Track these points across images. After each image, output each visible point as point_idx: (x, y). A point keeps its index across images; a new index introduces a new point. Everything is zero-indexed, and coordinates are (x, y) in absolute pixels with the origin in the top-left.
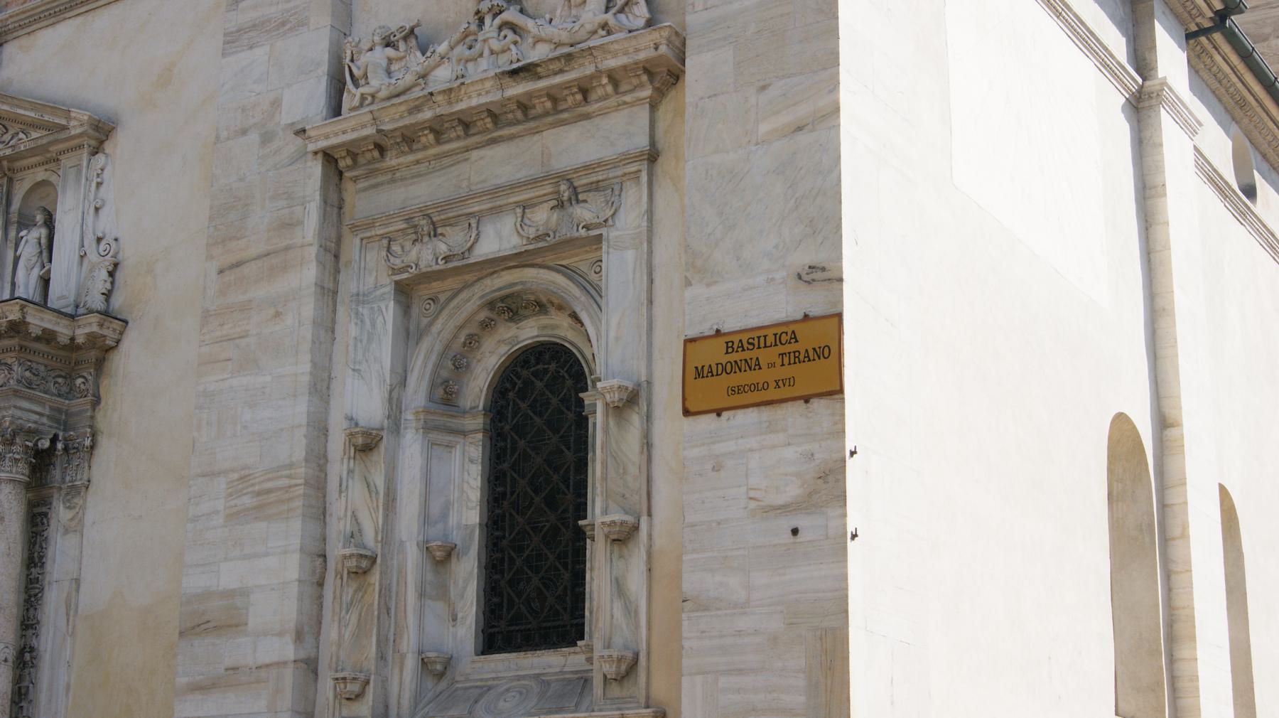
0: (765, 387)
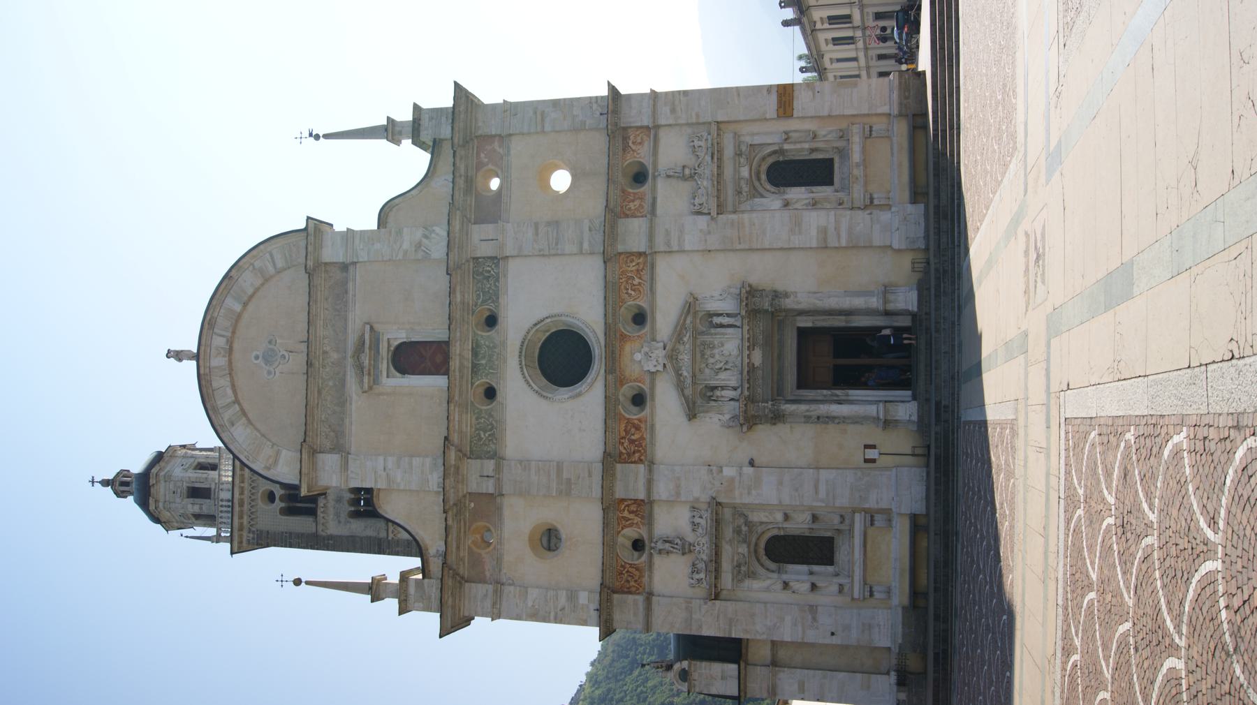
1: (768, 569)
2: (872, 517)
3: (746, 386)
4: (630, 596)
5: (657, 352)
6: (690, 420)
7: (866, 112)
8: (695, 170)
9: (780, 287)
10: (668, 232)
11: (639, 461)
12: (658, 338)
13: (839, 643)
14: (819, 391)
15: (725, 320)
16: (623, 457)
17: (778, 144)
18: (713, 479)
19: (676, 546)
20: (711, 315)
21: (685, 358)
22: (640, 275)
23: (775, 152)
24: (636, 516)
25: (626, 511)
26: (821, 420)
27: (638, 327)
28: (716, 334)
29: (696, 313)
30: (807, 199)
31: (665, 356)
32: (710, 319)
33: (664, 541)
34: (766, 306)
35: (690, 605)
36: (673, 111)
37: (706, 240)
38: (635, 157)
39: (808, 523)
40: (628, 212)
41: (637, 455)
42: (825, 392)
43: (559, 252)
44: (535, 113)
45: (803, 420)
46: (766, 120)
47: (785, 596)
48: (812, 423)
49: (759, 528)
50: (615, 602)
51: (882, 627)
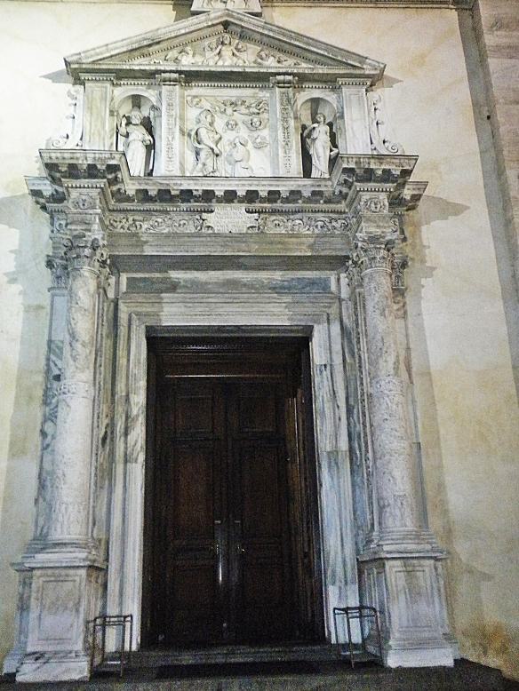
26: (55, 384)
28: (286, 129)
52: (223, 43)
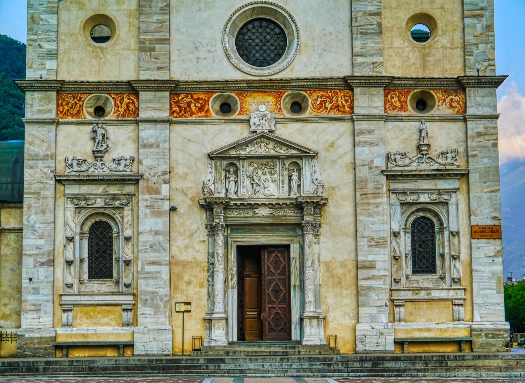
0: (487, 236)
1: (83, 224)
2: (131, 310)
3: (239, 203)
4: (54, 106)
5: (267, 124)
6: (209, 155)
7: (475, 302)
8: (426, 154)
9: (322, 231)
10: (370, 132)
11: (172, 111)
12: (279, 126)
13: (24, 285)
14: (236, 264)
15: (294, 184)
16: (175, 97)
17: (449, 227)
18: (159, 176)
19: (100, 145)
20: (299, 170)
21: (262, 149)
22: (334, 109)
23: (442, 224)
24: (125, 110)
25: (128, 101)
26: (211, 266)
27: (289, 107)
29: (300, 157)
30: (400, 251)
31: (263, 132)
32: (295, 170)
33: (104, 135)
34: (307, 219)
35: (50, 159)
36: (479, 134)
37: (364, 166)
38: (439, 101)
39: (123, 257)
40: (389, 96)
41: (177, 109)
42: (235, 269)
43: (354, 36)
44: (482, 9)
45: (211, 251)
46: (470, 216)
47: (60, 239)
48: (208, 258)
49: (118, 216)
50: (48, 93)
51: (38, 320)
52: (261, 142)
